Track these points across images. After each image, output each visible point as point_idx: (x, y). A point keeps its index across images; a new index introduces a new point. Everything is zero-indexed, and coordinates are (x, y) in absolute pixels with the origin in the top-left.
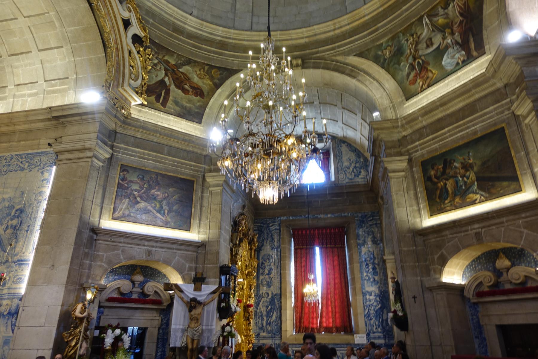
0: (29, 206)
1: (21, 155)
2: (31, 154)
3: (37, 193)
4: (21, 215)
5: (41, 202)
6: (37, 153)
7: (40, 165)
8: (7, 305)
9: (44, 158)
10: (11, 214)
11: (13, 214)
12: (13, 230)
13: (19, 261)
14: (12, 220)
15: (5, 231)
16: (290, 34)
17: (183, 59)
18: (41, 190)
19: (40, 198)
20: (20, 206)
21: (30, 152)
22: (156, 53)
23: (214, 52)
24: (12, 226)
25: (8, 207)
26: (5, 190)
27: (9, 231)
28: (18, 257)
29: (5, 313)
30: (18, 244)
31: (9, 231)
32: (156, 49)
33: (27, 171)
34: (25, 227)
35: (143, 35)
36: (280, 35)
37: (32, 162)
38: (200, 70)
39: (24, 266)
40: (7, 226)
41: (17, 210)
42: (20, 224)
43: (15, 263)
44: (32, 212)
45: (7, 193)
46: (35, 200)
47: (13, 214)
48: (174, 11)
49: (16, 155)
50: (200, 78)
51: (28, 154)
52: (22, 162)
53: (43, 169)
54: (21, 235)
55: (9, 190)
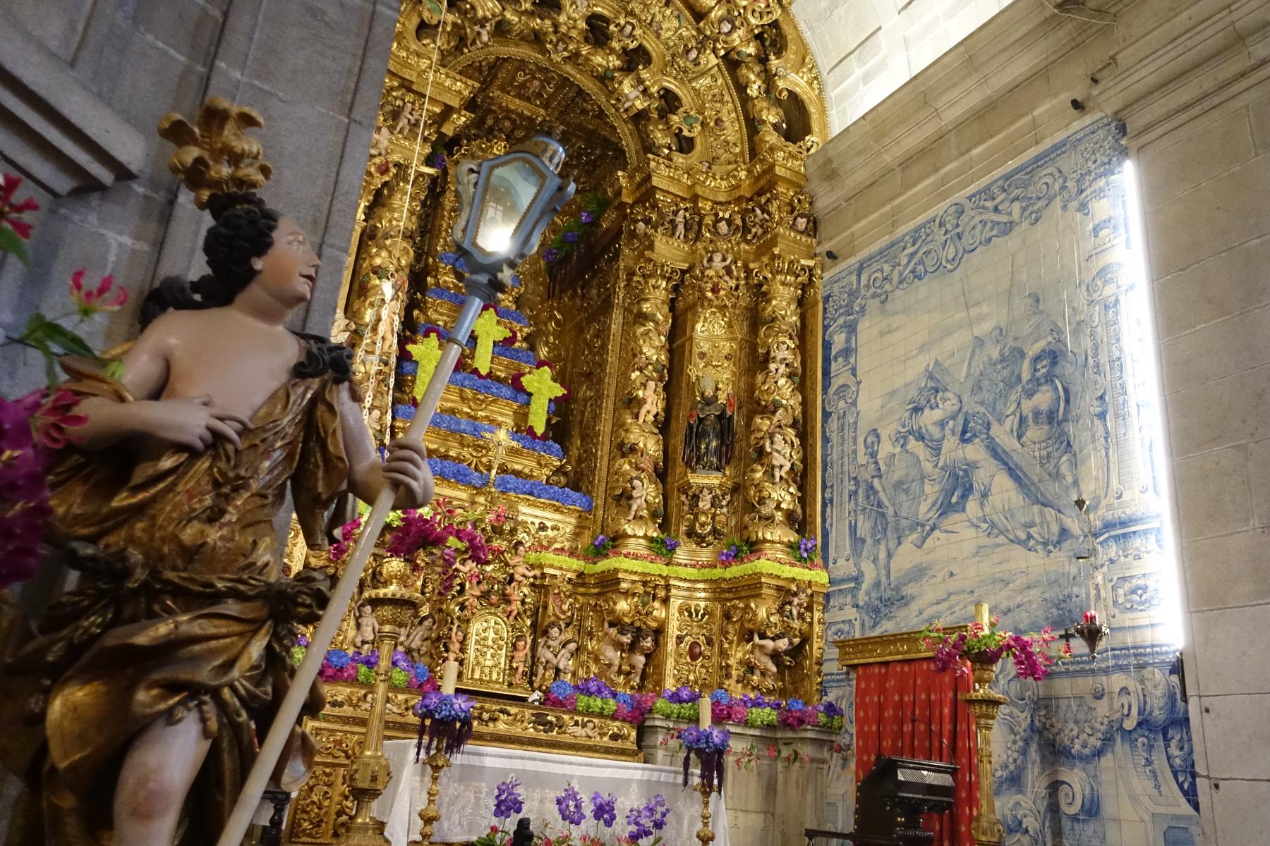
0: (1076, 332)
1: (988, 188)
2: (1018, 171)
3: (1088, 279)
4: (1058, 370)
5: (1117, 301)
6: (1038, 158)
7: (1063, 188)
8: (1124, 690)
9: (1069, 162)
10: (1019, 378)
11: (1026, 376)
12: (1046, 427)
13: (1108, 526)
14: (1030, 395)
15: (1019, 437)
18: (1101, 264)
19: (1109, 290)
20: (1041, 344)
21: (1012, 164)
24: (1037, 414)
25: (1003, 359)
26: (974, 312)
27: (1034, 433)
28: (1100, 512)
29: (1129, 724)
30: (1082, 469)
31: (1034, 433)
33: (1025, 225)
34: (1086, 404)
37: (1032, 192)
39: (1136, 542)
40: (1022, 420)
41: (1037, 359)
42: (1067, 401)
43: (1096, 535)
44: (1096, 348)
45: (981, 318)
46: (1090, 303)
47: (1026, 376)
49: (970, 198)
51: (1007, 177)
52: (996, 209)
53: (1078, 195)
54: (1086, 435)
55: (985, 309)
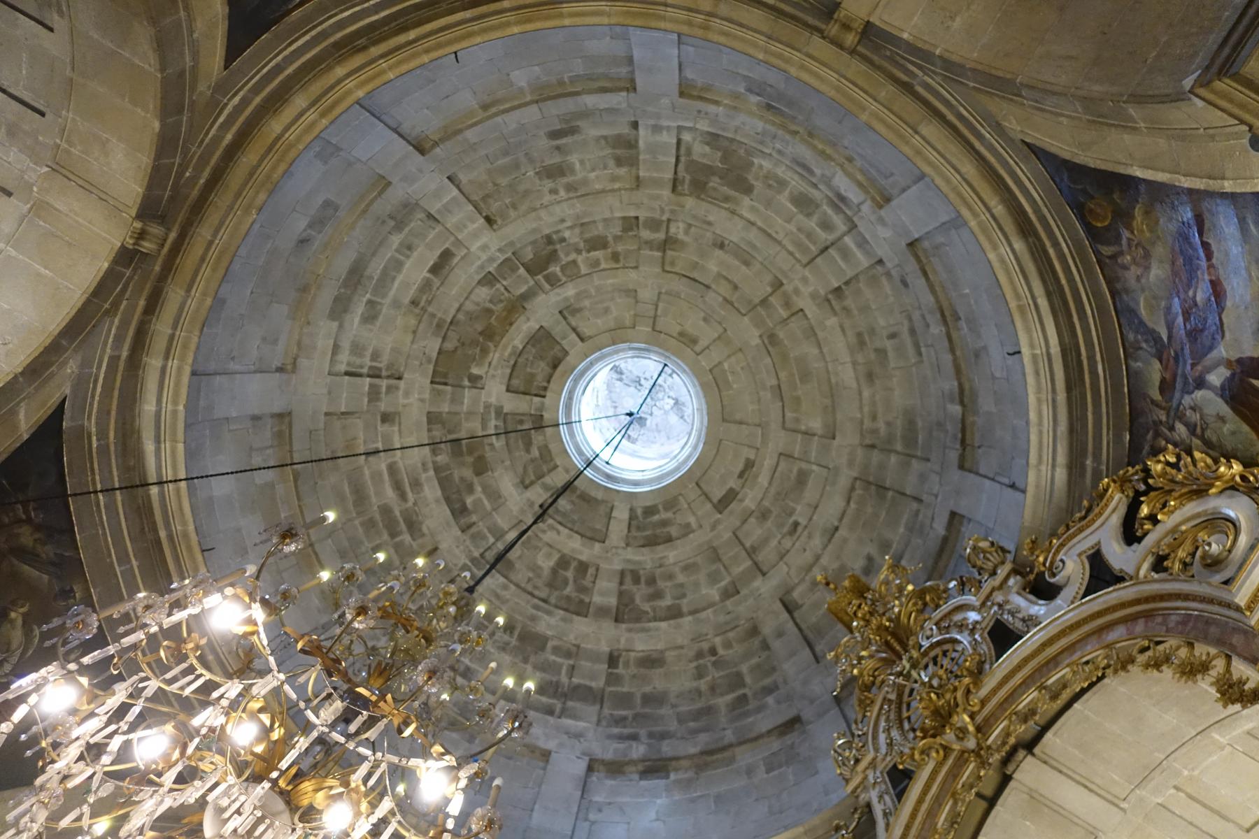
16: (837, 89)
17: (1131, 336)
22: (1157, 434)
23: (1056, 244)
32: (1150, 436)
35: (1117, 496)
36: (864, 109)
38: (1125, 268)
48: (1039, 400)
50: (1147, 255)
